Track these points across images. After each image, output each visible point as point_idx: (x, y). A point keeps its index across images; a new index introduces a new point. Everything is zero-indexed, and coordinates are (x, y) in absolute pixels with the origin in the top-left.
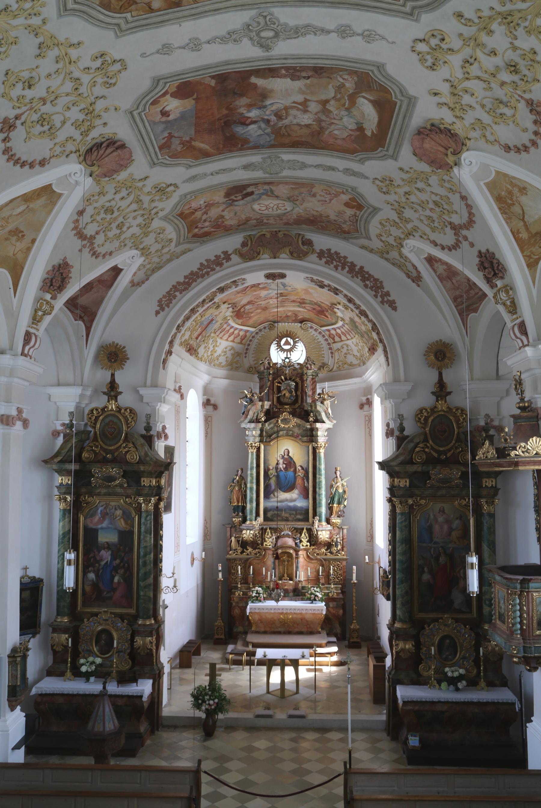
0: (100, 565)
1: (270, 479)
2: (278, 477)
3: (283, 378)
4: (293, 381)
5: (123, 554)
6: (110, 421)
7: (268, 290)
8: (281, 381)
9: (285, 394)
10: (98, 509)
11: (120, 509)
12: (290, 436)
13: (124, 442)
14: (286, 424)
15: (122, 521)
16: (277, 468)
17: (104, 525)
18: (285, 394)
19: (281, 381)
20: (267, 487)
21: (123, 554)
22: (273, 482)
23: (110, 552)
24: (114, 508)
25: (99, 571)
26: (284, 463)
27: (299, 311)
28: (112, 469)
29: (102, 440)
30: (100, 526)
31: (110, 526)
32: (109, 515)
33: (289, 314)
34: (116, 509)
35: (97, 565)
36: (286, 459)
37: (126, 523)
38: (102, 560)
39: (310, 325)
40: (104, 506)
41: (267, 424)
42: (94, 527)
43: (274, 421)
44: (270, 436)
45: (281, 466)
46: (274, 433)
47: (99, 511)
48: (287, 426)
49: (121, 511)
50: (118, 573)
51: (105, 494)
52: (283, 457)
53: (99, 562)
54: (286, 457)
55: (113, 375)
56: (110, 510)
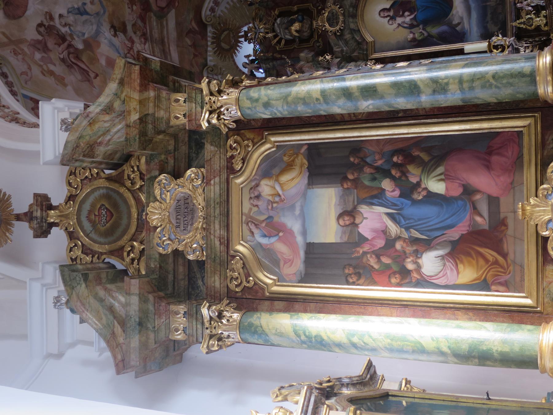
0: (398, 238)
1: (430, 36)
2: (426, 23)
3: (270, 35)
4: (276, 20)
5: (367, 170)
6: (90, 221)
7: (99, 44)
8: (277, 39)
9: (296, 31)
10: (260, 244)
11: (257, 185)
12: (357, 10)
13: (123, 185)
14: (337, 18)
15: (284, 178)
16: (411, 27)
17: (295, 226)
18: (296, 31)
19: (277, 39)
20: (444, 39)
21: (367, 170)
22: (434, 30)
23: (364, 209)
24: (255, 202)
25: (415, 241)
26: (402, 16)
27: (178, 24)
28: (156, 200)
29: (120, 238)
30: (299, 239)
31: (297, 212)
32: (272, 213)
33: (188, 41)
34: (258, 197)
35: (398, 246)
36: (395, 12)
37: (289, 167)
38: (385, 232)
39: (208, 13)
40: (253, 227)
41: (336, 49)
42: (302, 254)
43: (332, 40)
44: (359, 43)
45: (408, 19)
46: (353, 38)
47: (264, 241)
48: (341, 18)
49: (264, 182)
50: (418, 184)
51: (227, 227)
52: (393, 18)
53: (390, 243)
54: (391, 13)
55: (18, 218)
56: (260, 213)
